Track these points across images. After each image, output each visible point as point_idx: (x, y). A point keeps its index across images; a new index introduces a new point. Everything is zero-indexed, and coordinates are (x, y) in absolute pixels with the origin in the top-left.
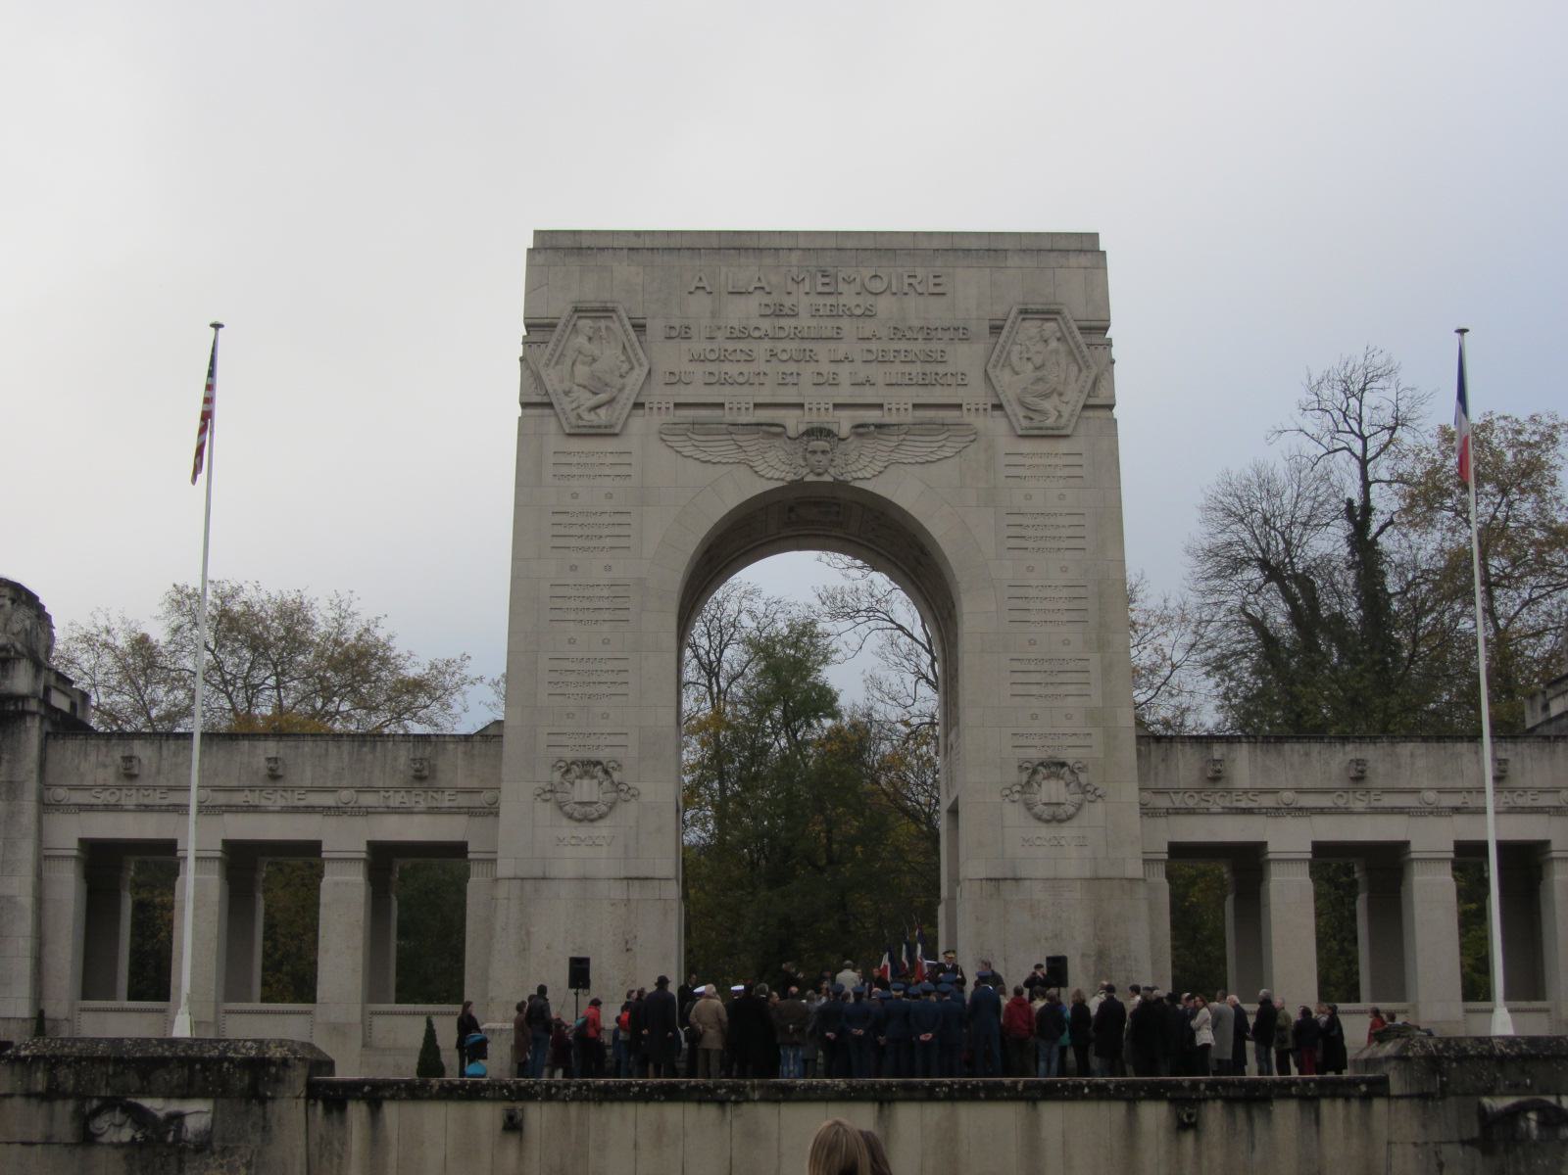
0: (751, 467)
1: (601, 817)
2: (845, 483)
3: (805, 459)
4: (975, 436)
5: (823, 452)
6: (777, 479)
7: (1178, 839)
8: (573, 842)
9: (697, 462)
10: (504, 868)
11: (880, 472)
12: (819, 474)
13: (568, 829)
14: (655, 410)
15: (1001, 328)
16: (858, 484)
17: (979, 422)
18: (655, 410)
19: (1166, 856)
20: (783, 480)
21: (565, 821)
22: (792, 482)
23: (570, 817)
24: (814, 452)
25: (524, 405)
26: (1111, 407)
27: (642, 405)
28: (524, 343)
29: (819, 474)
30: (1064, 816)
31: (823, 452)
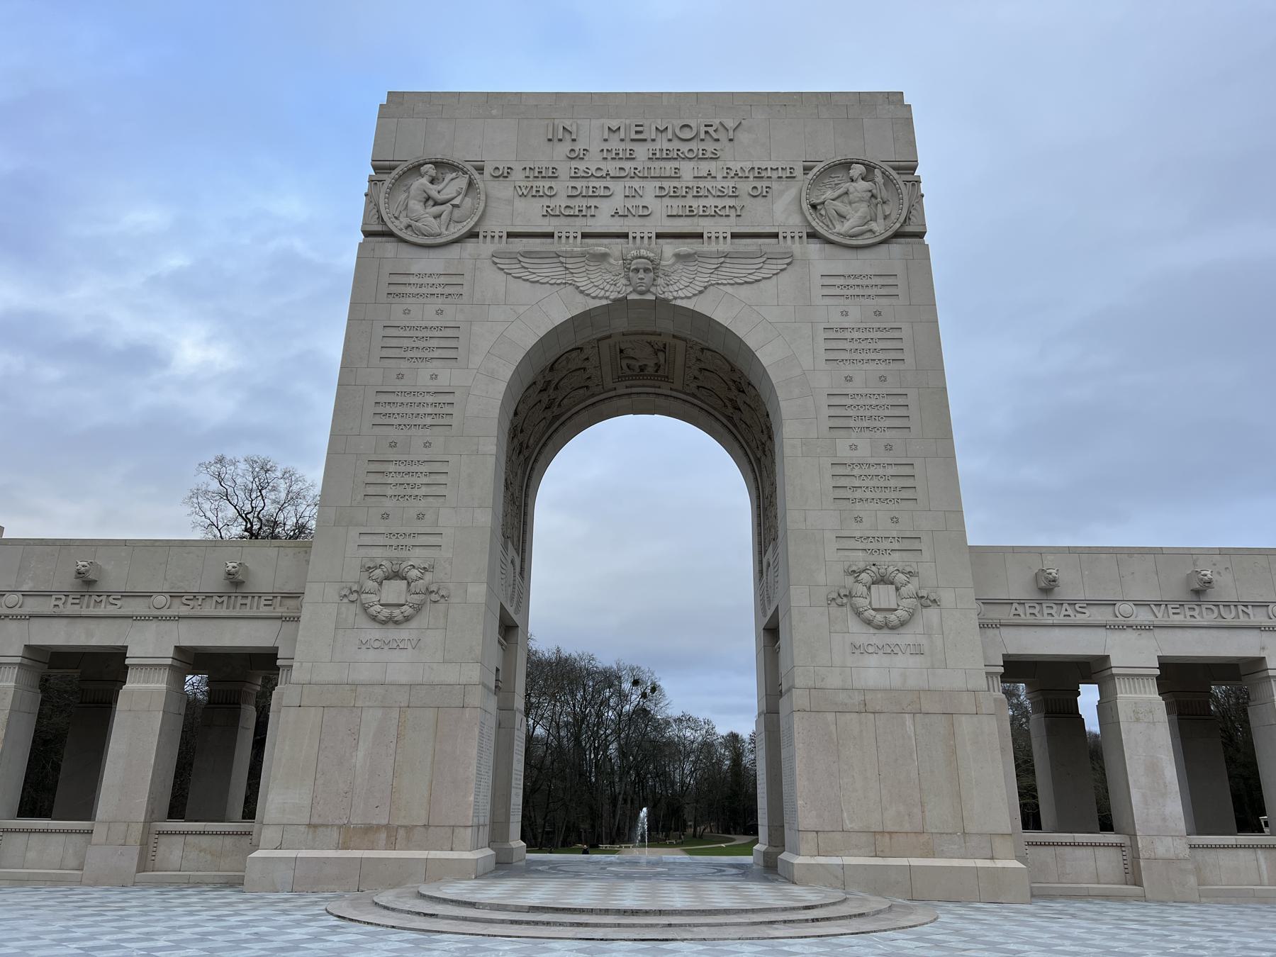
0: (578, 288)
1: (407, 619)
2: (666, 301)
3: (629, 279)
4: (791, 260)
5: (646, 270)
6: (601, 298)
7: (1013, 650)
8: (377, 644)
9: (528, 284)
10: (296, 675)
11: (701, 292)
12: (642, 293)
13: (374, 633)
14: (489, 238)
15: (811, 168)
16: (679, 302)
17: (796, 248)
18: (489, 238)
19: (1002, 670)
20: (607, 298)
21: (363, 622)
22: (615, 300)
23: (374, 618)
24: (637, 270)
25: (367, 234)
26: (921, 235)
27: (476, 235)
28: (371, 181)
29: (642, 293)
30: (896, 622)
31: (646, 270)
